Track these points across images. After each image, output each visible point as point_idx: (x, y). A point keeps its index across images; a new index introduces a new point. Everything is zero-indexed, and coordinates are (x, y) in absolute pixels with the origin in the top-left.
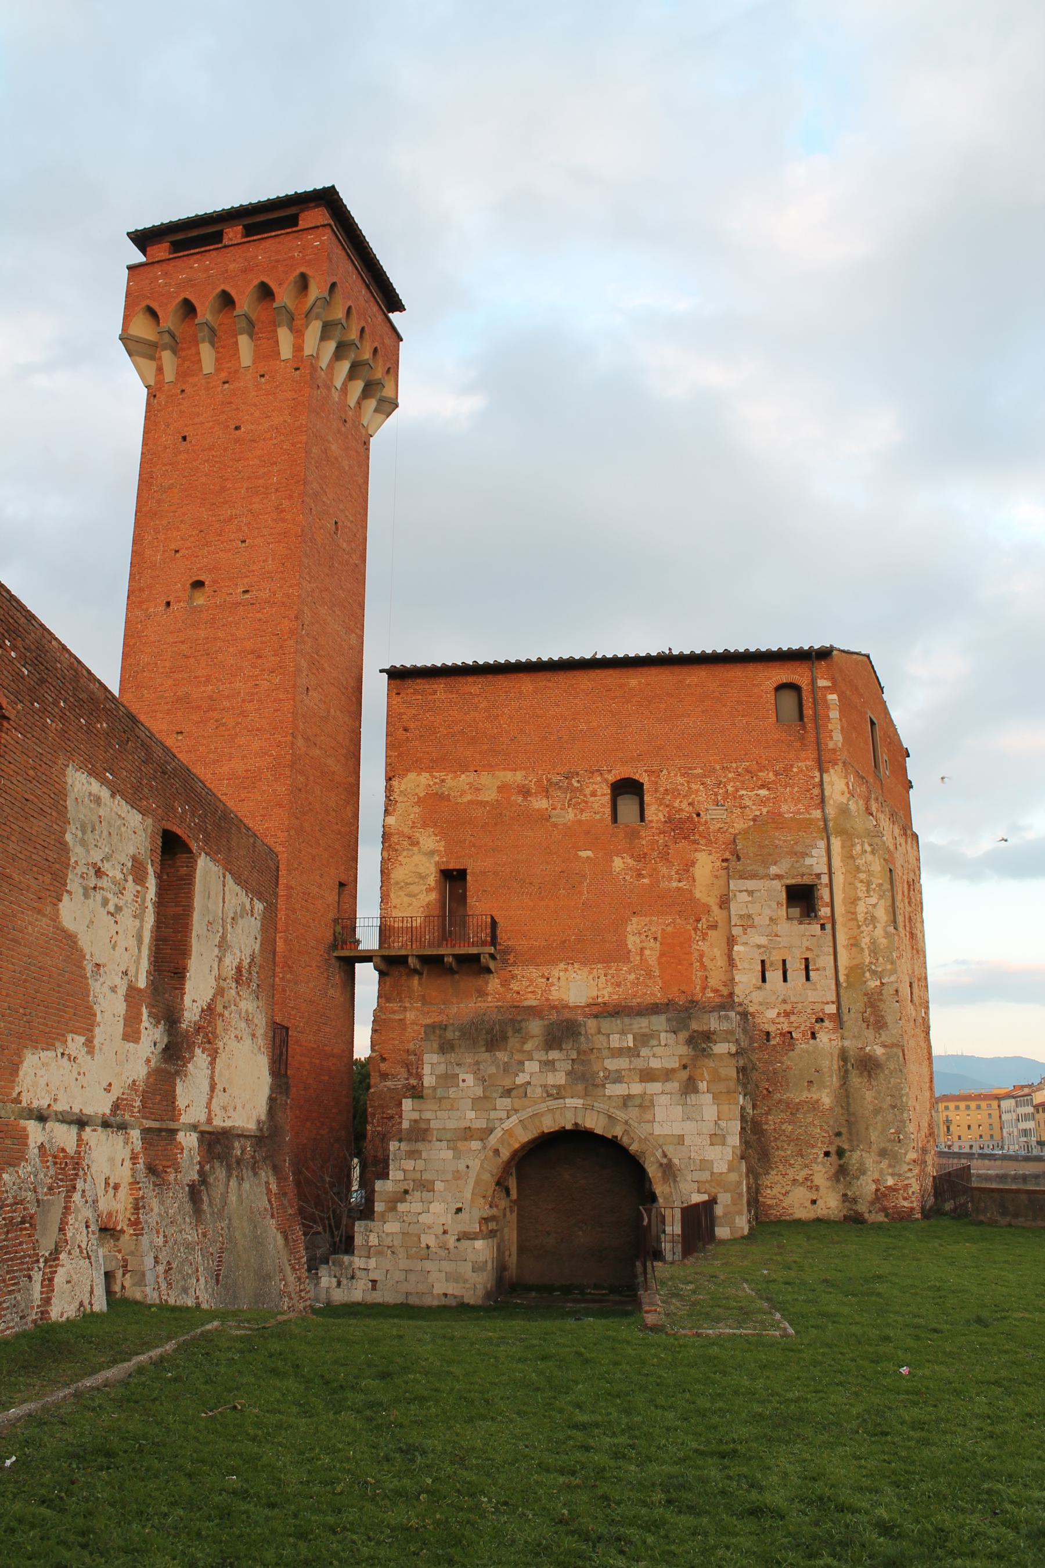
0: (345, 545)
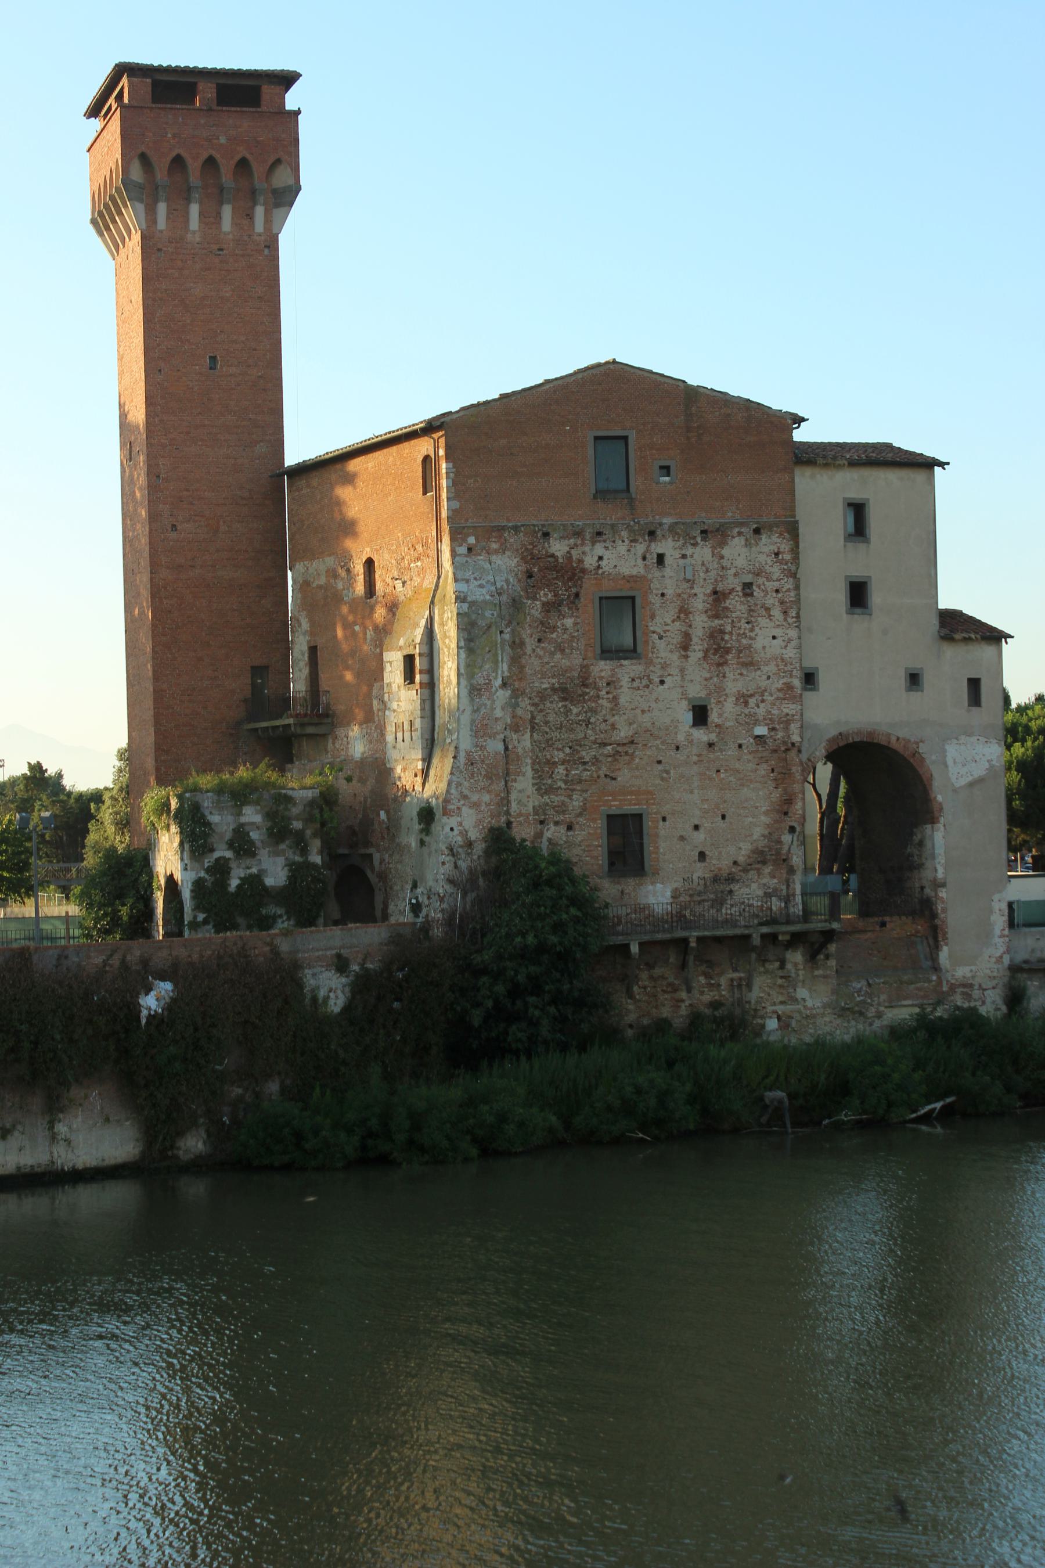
0: (233, 370)
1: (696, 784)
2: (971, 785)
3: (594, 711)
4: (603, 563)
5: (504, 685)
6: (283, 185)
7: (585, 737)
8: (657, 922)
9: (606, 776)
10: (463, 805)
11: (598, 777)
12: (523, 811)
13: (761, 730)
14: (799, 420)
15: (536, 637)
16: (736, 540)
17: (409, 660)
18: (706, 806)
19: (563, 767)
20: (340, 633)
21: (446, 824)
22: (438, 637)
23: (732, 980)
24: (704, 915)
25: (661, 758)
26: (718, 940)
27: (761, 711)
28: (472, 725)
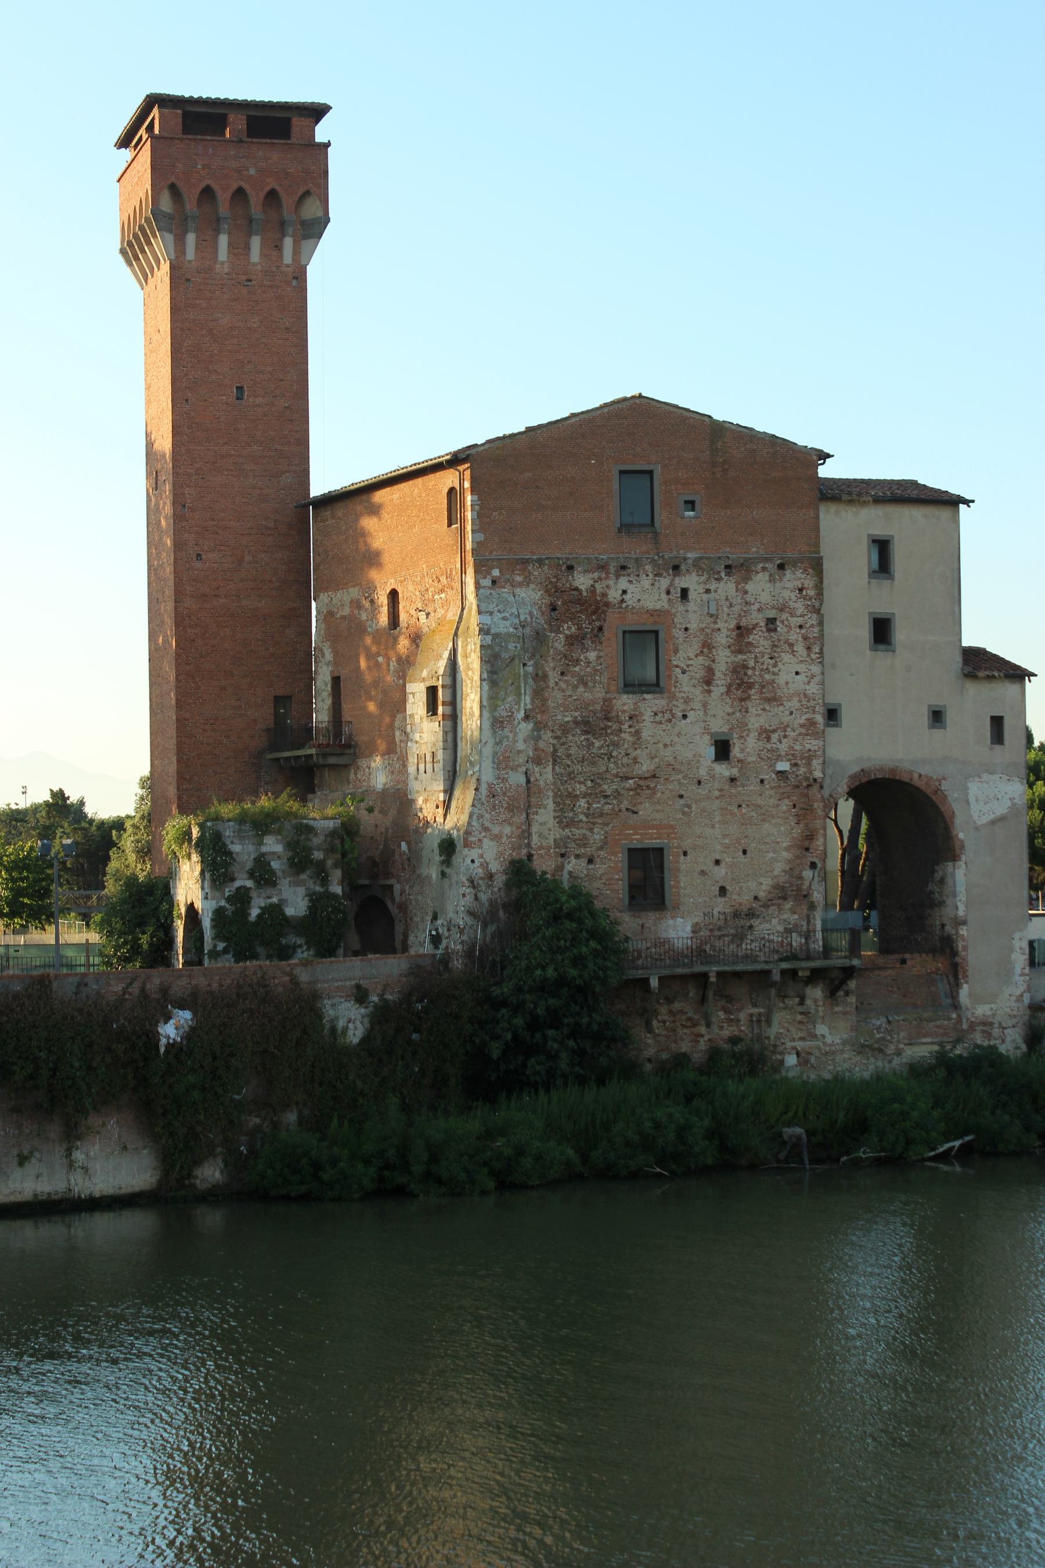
1: (717, 819)
2: (993, 822)
3: (616, 745)
4: (627, 597)
5: (527, 717)
6: (312, 217)
7: (607, 771)
8: (677, 957)
9: (627, 809)
10: (484, 837)
11: (620, 811)
12: (544, 844)
13: (783, 766)
14: (824, 456)
15: (559, 670)
16: (761, 574)
17: (432, 691)
18: (727, 841)
19: (584, 800)
20: (363, 663)
21: (466, 856)
22: (461, 668)
23: (751, 1015)
24: (724, 950)
25: (683, 793)
26: (738, 975)
27: (783, 747)
28: (494, 757)
